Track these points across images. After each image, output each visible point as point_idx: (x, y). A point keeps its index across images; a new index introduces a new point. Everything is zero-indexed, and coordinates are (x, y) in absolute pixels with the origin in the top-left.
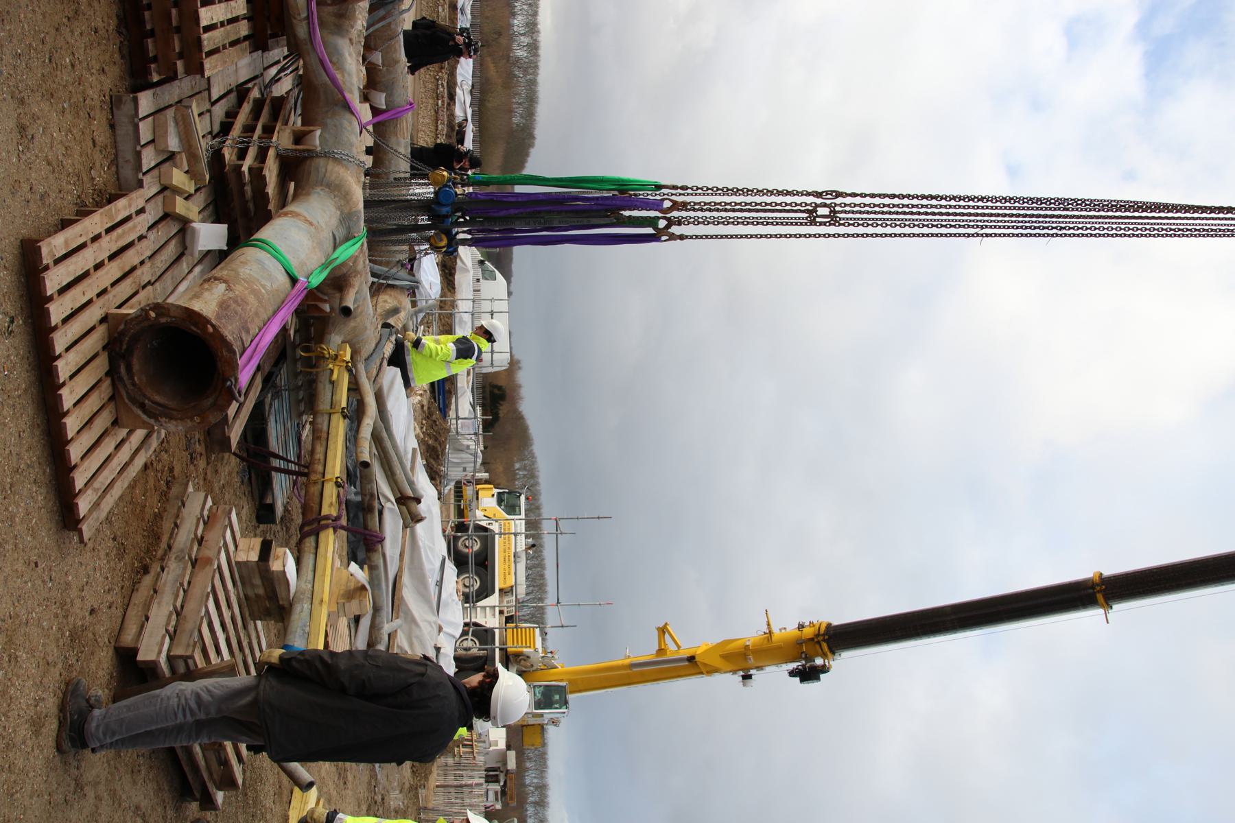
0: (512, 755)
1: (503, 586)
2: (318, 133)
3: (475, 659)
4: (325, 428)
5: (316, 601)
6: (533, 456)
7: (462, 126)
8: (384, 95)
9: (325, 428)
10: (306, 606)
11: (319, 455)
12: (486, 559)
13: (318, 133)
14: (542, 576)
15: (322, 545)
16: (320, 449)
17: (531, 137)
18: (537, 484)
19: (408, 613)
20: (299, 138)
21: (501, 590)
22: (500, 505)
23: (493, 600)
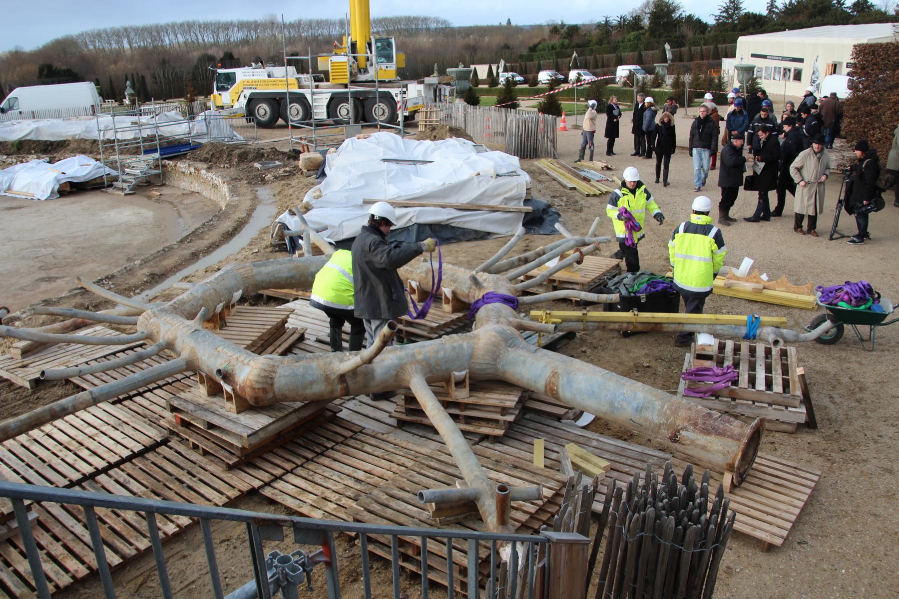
0: (427, 80)
1: (297, 86)
2: (457, 373)
3: (356, 107)
4: (596, 324)
5: (717, 322)
6: (82, 35)
8: (235, 294)
9: (596, 324)
10: (719, 327)
11: (617, 326)
12: (275, 99)
13: (457, 373)
14: (182, 25)
15: (690, 321)
16: (612, 326)
18: (105, 31)
19: (477, 199)
20: (460, 384)
21: (300, 87)
22: (227, 89)
23: (307, 93)
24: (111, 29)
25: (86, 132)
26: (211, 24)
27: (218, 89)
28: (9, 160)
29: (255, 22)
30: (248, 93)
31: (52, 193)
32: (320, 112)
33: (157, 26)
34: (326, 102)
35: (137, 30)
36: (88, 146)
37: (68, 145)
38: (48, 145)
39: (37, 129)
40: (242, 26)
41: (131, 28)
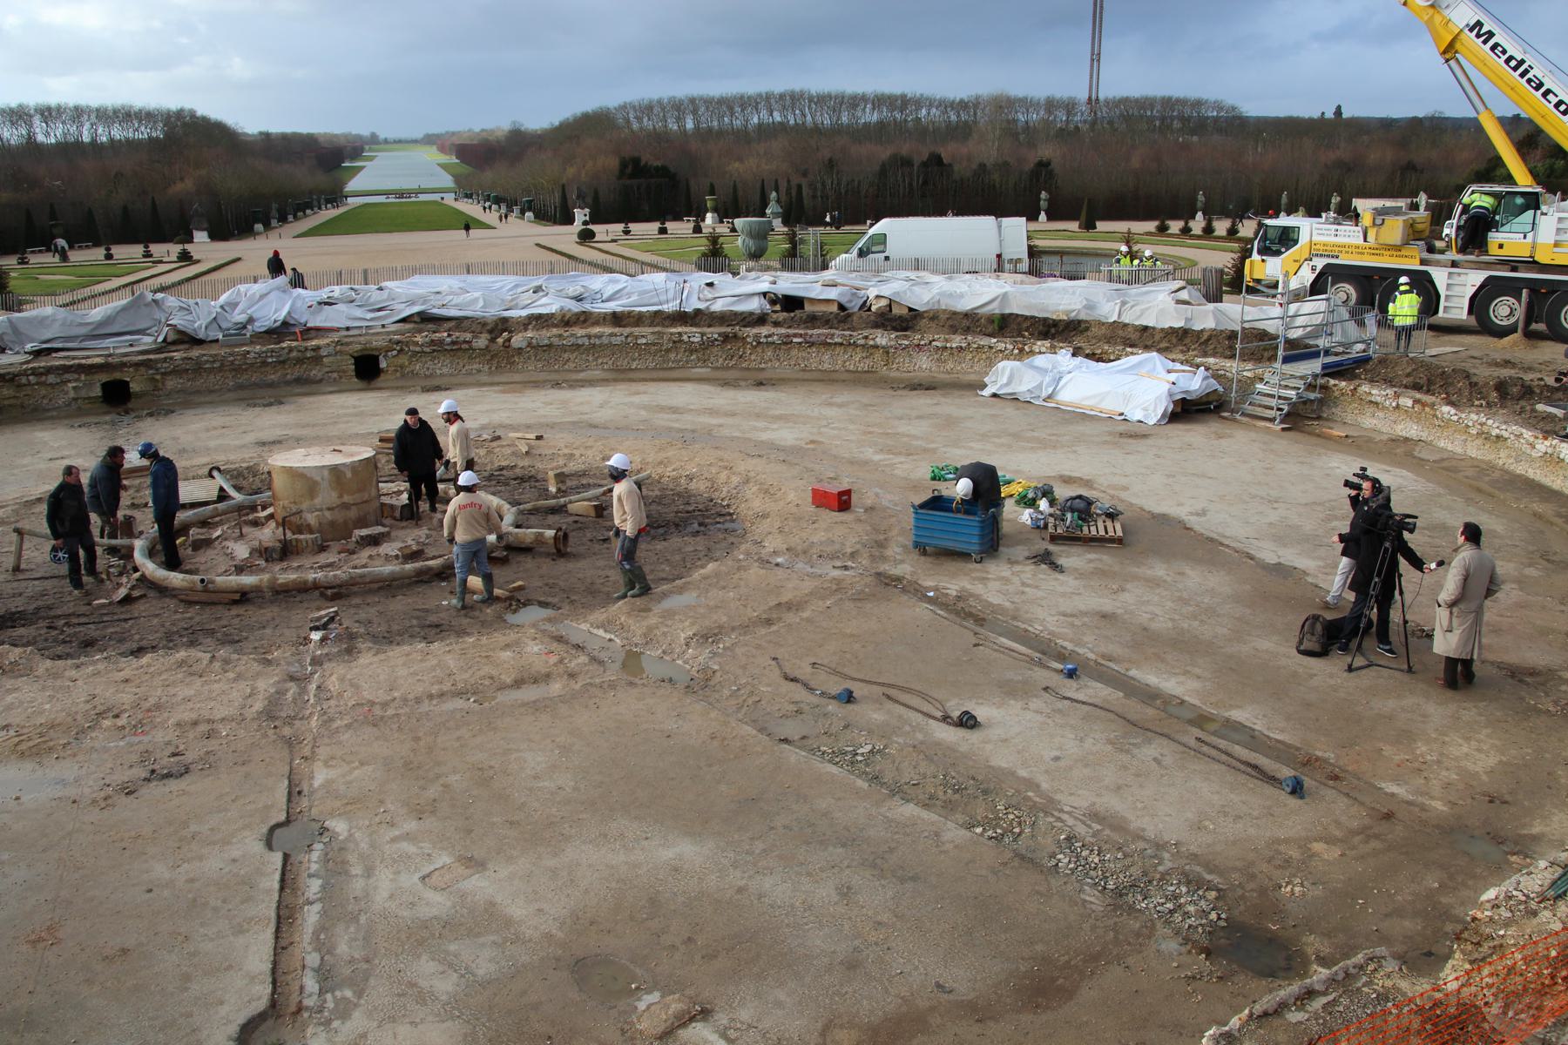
6: (624, 107)
7: (774, 299)
14: (782, 96)
17: (180, 114)
18: (660, 102)
22: (1278, 253)
24: (670, 100)
25: (1090, 306)
26: (830, 96)
27: (1259, 252)
28: (1001, 346)
29: (903, 97)
30: (1320, 263)
31: (1163, 416)
32: (1455, 307)
33: (742, 97)
34: (1470, 291)
35: (708, 102)
36: (1134, 336)
37: (1087, 329)
38: (1049, 326)
39: (1005, 295)
40: (880, 101)
41: (701, 99)
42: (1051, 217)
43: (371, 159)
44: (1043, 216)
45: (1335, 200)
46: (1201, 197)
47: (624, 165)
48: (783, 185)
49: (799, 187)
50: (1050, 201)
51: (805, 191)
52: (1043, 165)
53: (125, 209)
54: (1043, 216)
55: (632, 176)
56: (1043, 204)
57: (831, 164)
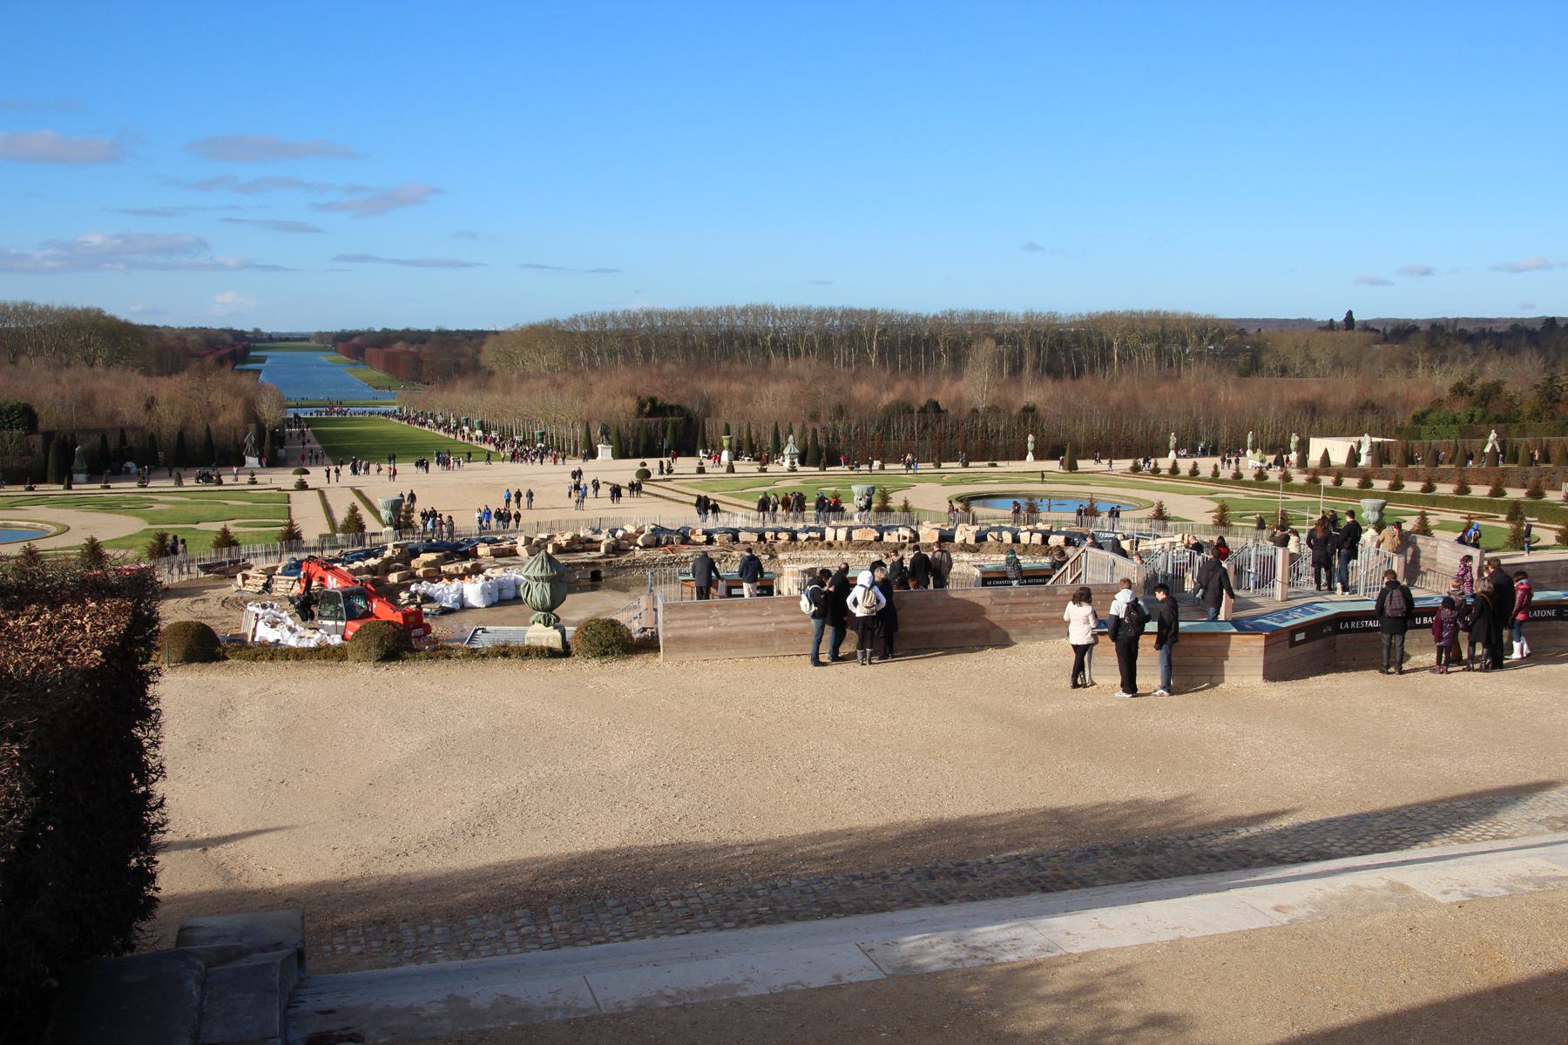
17: (87, 312)
18: (613, 315)
42: (1039, 456)
43: (262, 360)
44: (1030, 456)
45: (1295, 439)
46: (1173, 439)
47: (642, 405)
48: (797, 429)
49: (815, 431)
50: (1035, 442)
51: (819, 434)
52: (1029, 410)
53: (181, 435)
54: (1030, 456)
55: (649, 415)
56: (1030, 446)
57: (840, 411)
